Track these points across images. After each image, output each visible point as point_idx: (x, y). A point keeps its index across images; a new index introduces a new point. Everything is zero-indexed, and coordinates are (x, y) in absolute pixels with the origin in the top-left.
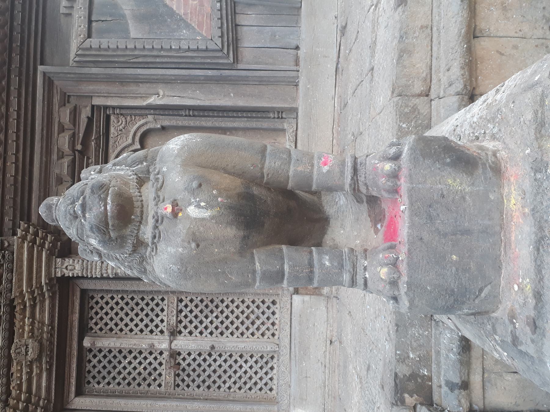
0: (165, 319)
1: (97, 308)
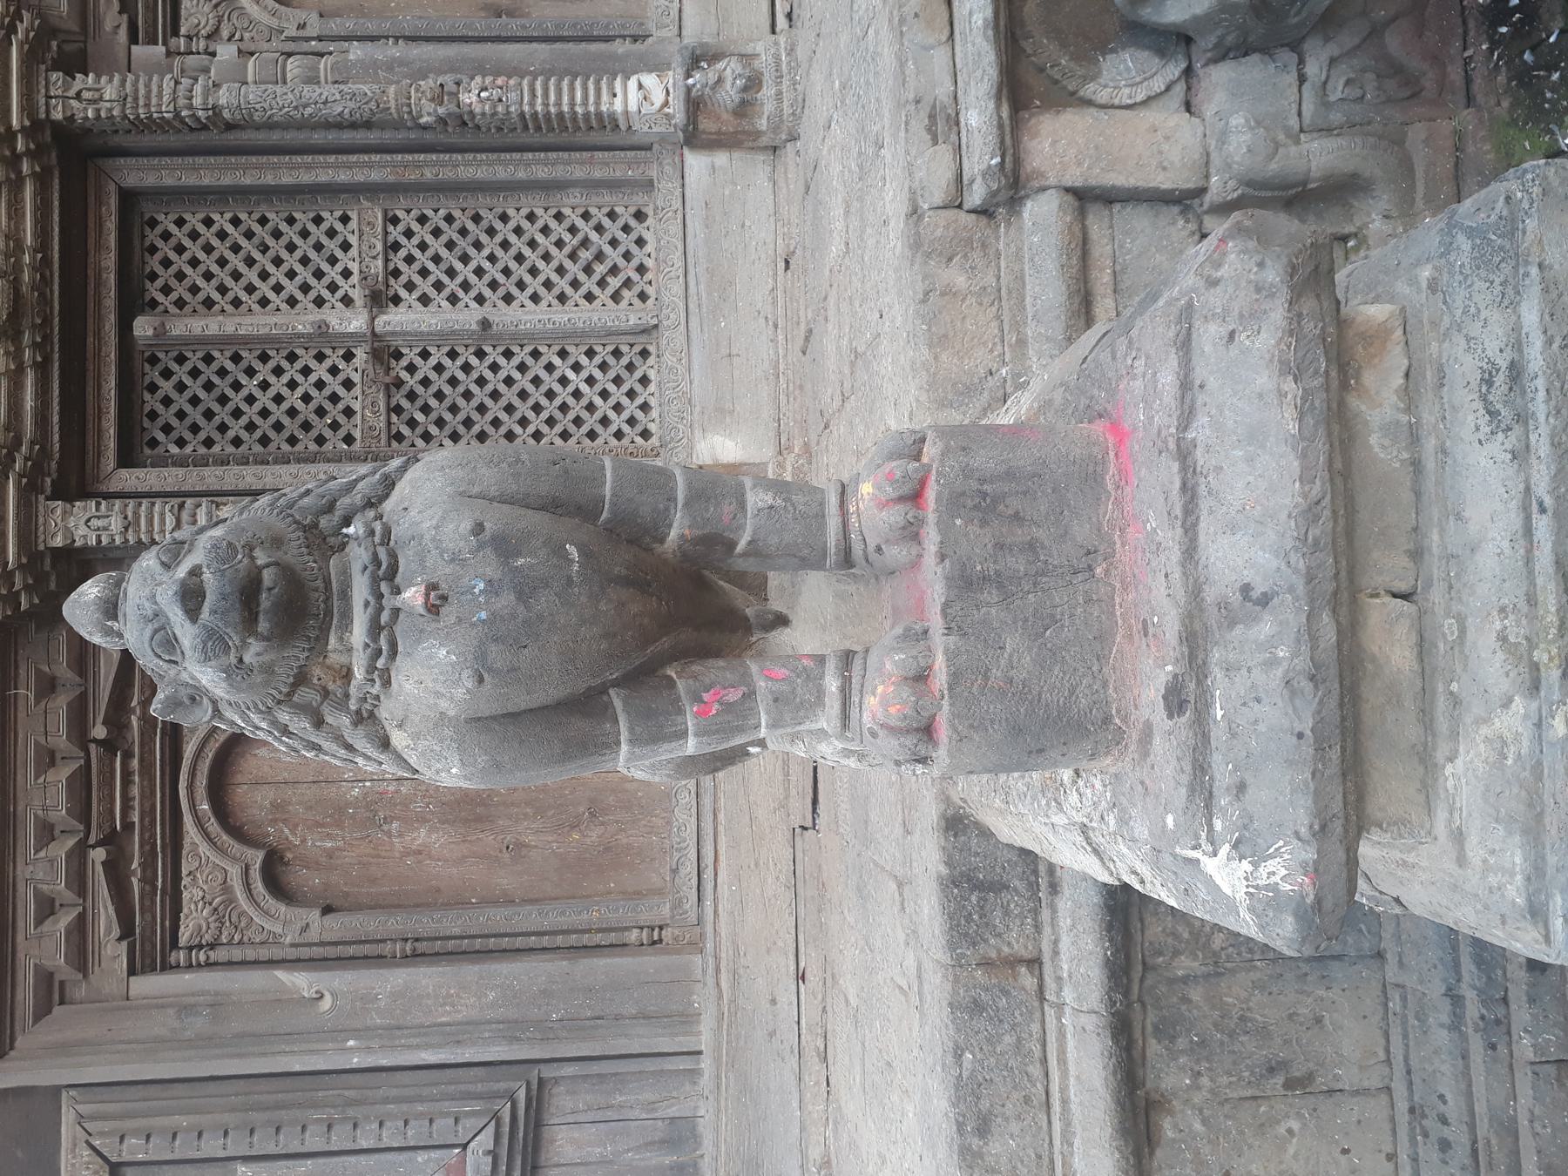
0: (354, 267)
1: (165, 276)
